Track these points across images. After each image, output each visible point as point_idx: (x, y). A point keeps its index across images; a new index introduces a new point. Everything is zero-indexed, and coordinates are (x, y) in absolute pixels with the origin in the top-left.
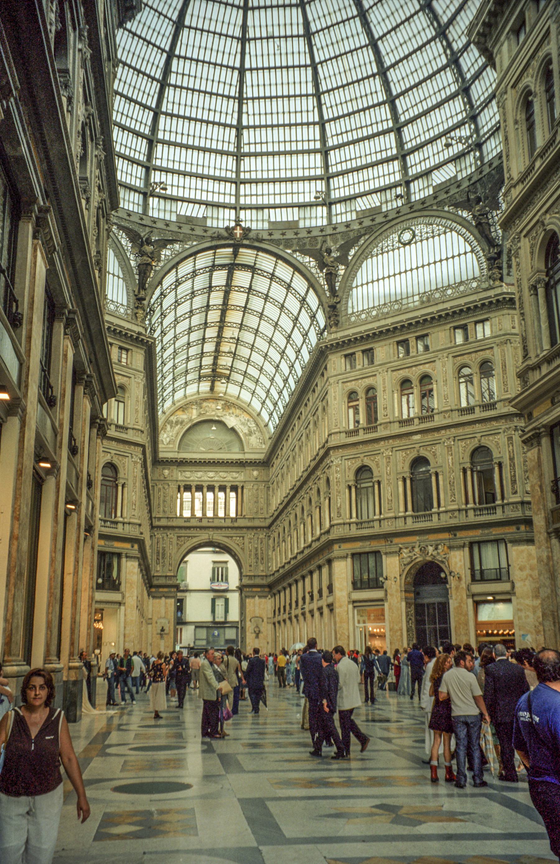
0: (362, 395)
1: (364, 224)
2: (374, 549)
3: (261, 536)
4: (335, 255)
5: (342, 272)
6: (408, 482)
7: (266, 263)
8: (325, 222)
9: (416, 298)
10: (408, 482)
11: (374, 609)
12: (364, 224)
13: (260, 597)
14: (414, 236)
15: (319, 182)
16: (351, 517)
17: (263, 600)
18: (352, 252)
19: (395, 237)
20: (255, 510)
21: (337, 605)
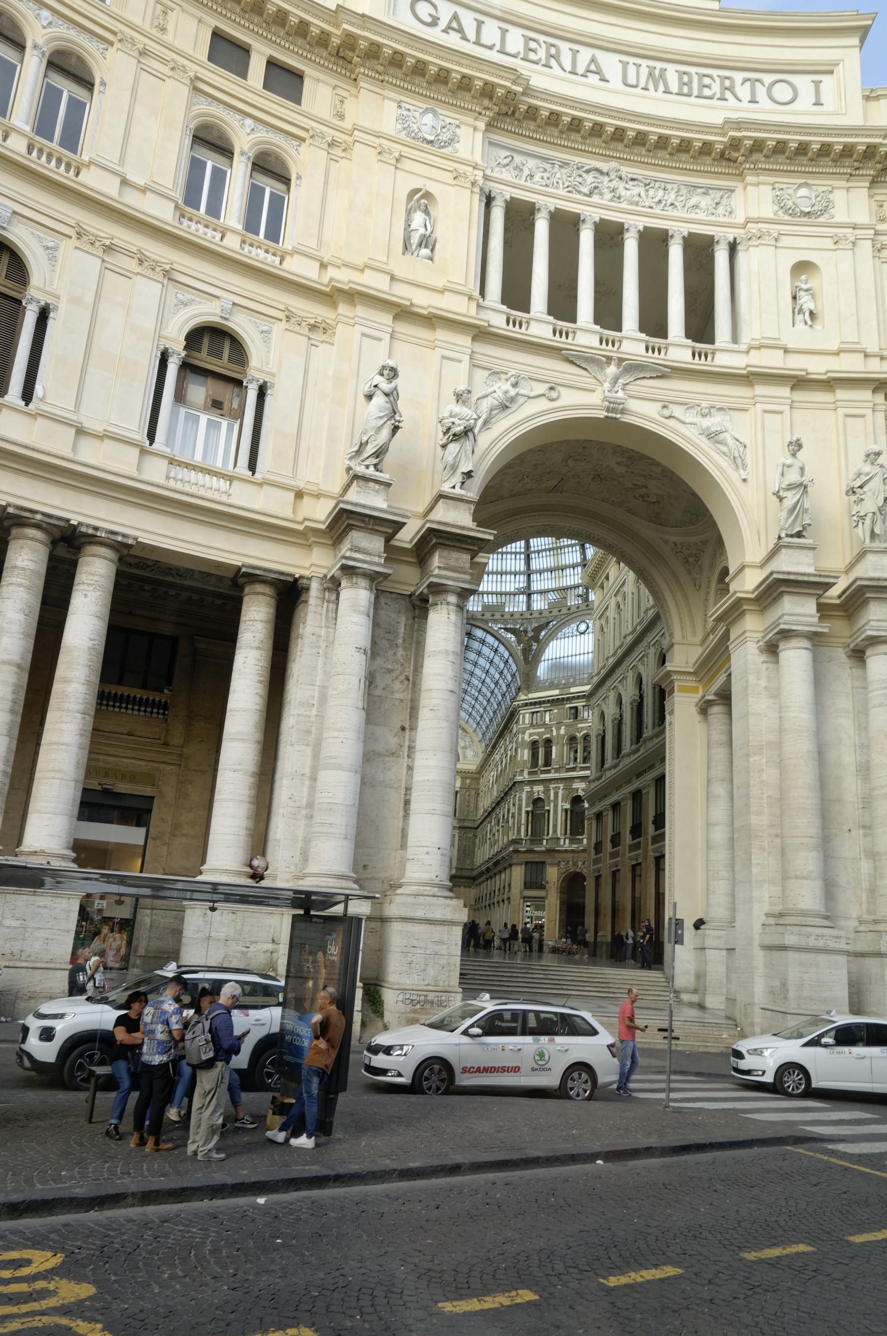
0: (541, 744)
1: (553, 614)
2: (542, 860)
3: (470, 835)
4: (530, 634)
5: (534, 648)
6: (569, 813)
7: (479, 633)
8: (524, 609)
9: (586, 676)
10: (569, 813)
11: (539, 904)
12: (553, 614)
13: (465, 887)
14: (588, 627)
15: (522, 576)
16: (527, 835)
17: (467, 890)
18: (543, 633)
19: (574, 626)
20: (466, 813)
21: (512, 899)
